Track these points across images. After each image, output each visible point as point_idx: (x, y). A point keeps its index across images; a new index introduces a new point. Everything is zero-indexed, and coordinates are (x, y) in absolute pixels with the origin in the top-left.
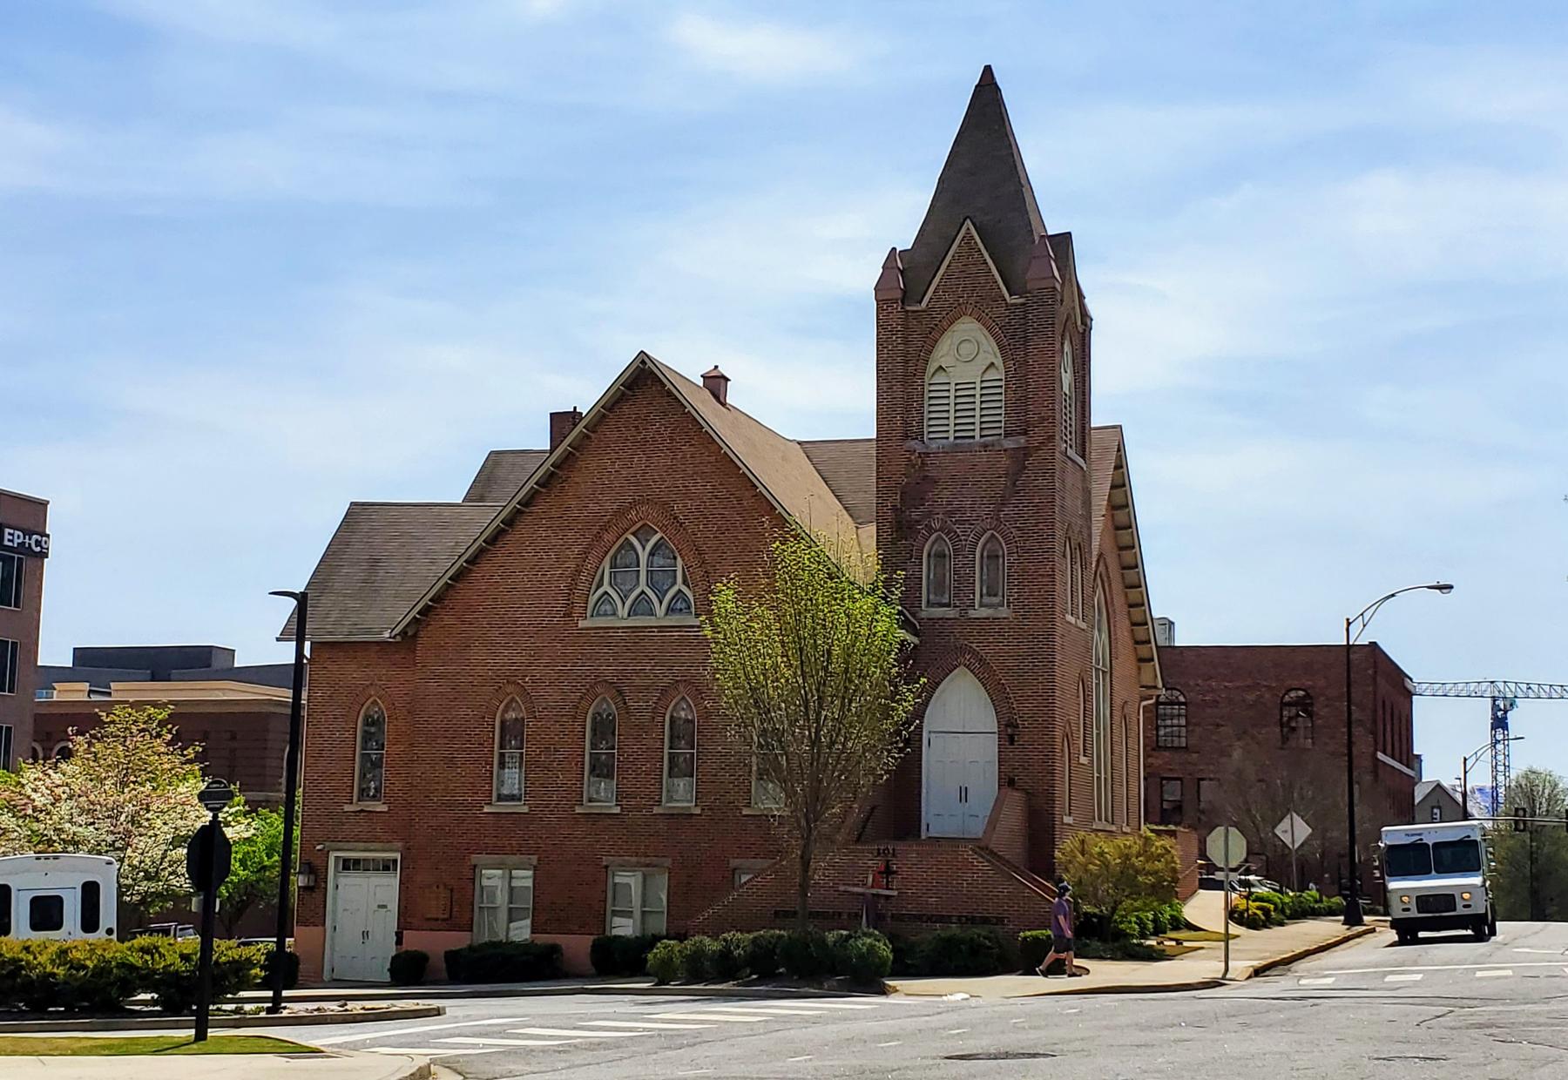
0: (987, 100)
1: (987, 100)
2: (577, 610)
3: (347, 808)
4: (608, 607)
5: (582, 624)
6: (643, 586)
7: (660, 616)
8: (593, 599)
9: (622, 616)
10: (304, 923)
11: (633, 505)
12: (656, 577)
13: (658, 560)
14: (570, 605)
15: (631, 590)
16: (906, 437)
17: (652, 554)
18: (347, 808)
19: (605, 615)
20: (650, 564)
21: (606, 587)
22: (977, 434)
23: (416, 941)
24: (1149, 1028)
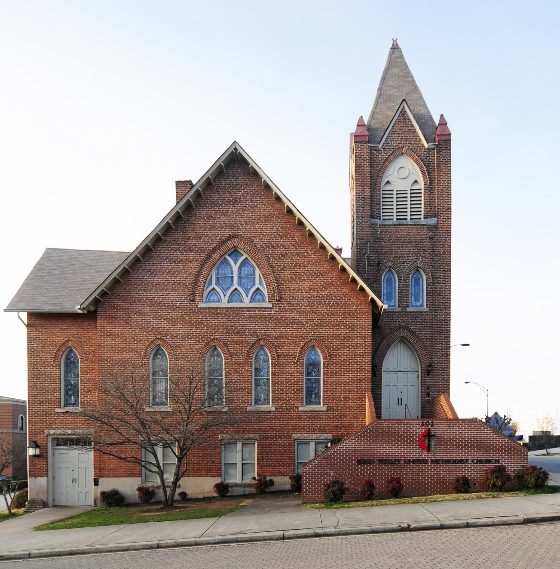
0: (395, 48)
1: (395, 48)
2: (197, 298)
3: (57, 410)
4: (215, 298)
5: (201, 305)
6: (236, 285)
7: (246, 302)
8: (206, 293)
9: (224, 303)
10: (34, 475)
11: (230, 238)
12: (243, 281)
13: (245, 269)
14: (194, 294)
15: (228, 288)
16: (372, 217)
17: (240, 268)
18: (57, 410)
19: (214, 301)
20: (240, 272)
21: (214, 285)
22: (409, 218)
23: (109, 484)
24: (237, 534)
